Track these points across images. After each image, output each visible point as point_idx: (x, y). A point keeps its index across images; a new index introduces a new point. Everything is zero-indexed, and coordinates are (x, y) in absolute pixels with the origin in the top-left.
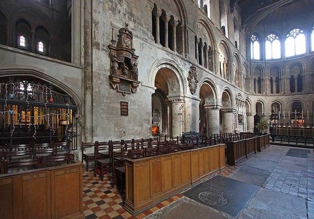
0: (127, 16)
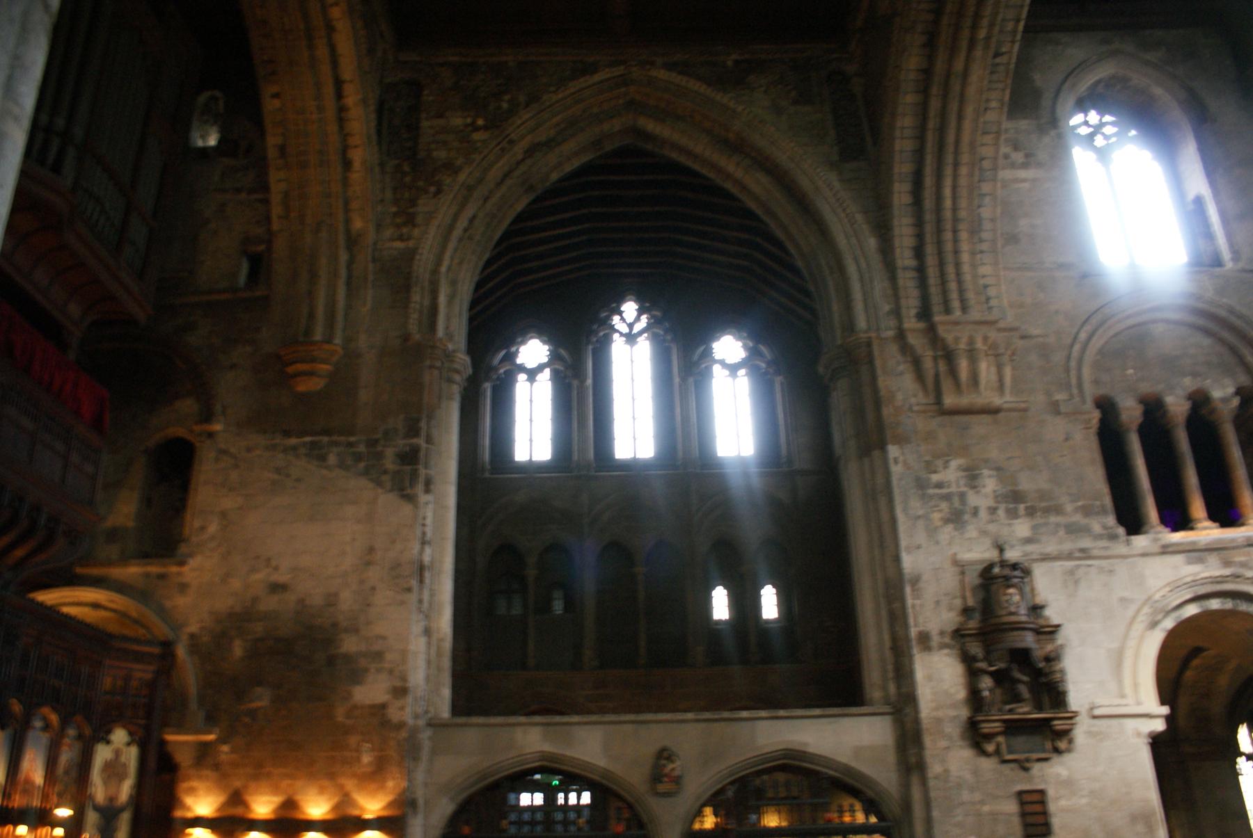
0: (1001, 512)
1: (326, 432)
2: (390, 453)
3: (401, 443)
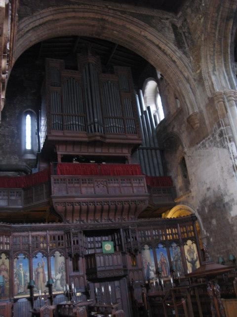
1: (204, 138)
2: (217, 136)
3: (218, 131)
